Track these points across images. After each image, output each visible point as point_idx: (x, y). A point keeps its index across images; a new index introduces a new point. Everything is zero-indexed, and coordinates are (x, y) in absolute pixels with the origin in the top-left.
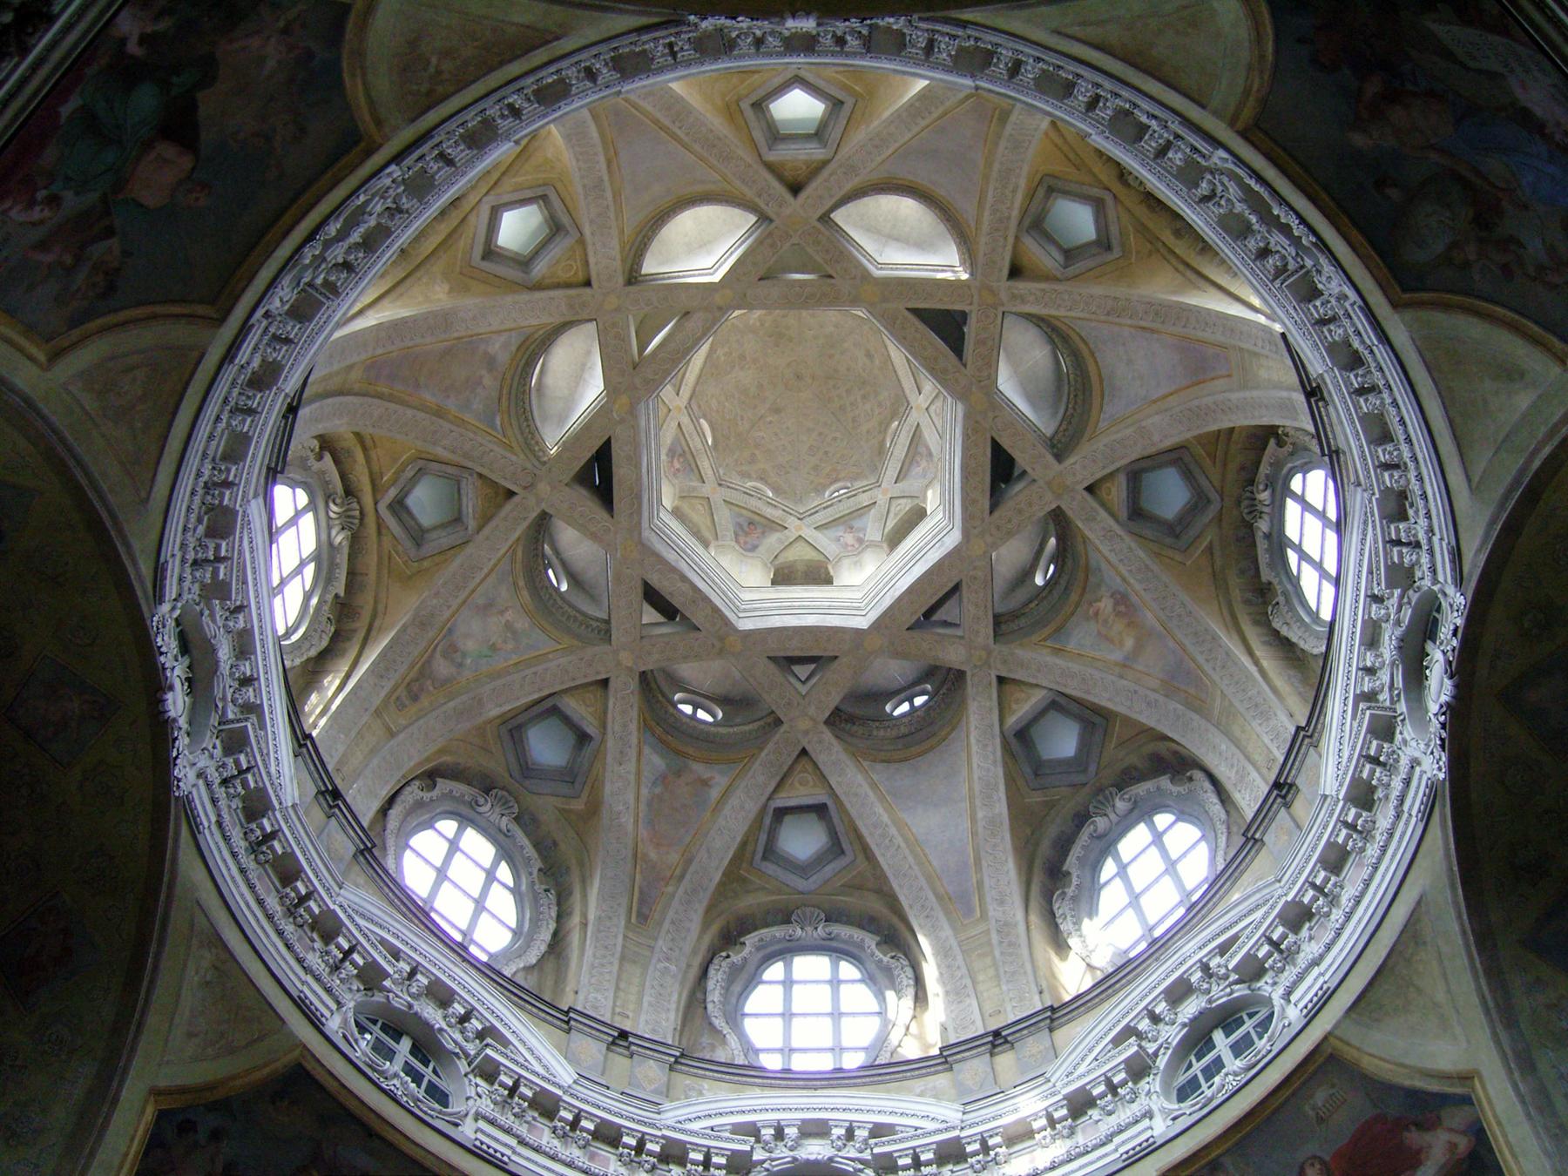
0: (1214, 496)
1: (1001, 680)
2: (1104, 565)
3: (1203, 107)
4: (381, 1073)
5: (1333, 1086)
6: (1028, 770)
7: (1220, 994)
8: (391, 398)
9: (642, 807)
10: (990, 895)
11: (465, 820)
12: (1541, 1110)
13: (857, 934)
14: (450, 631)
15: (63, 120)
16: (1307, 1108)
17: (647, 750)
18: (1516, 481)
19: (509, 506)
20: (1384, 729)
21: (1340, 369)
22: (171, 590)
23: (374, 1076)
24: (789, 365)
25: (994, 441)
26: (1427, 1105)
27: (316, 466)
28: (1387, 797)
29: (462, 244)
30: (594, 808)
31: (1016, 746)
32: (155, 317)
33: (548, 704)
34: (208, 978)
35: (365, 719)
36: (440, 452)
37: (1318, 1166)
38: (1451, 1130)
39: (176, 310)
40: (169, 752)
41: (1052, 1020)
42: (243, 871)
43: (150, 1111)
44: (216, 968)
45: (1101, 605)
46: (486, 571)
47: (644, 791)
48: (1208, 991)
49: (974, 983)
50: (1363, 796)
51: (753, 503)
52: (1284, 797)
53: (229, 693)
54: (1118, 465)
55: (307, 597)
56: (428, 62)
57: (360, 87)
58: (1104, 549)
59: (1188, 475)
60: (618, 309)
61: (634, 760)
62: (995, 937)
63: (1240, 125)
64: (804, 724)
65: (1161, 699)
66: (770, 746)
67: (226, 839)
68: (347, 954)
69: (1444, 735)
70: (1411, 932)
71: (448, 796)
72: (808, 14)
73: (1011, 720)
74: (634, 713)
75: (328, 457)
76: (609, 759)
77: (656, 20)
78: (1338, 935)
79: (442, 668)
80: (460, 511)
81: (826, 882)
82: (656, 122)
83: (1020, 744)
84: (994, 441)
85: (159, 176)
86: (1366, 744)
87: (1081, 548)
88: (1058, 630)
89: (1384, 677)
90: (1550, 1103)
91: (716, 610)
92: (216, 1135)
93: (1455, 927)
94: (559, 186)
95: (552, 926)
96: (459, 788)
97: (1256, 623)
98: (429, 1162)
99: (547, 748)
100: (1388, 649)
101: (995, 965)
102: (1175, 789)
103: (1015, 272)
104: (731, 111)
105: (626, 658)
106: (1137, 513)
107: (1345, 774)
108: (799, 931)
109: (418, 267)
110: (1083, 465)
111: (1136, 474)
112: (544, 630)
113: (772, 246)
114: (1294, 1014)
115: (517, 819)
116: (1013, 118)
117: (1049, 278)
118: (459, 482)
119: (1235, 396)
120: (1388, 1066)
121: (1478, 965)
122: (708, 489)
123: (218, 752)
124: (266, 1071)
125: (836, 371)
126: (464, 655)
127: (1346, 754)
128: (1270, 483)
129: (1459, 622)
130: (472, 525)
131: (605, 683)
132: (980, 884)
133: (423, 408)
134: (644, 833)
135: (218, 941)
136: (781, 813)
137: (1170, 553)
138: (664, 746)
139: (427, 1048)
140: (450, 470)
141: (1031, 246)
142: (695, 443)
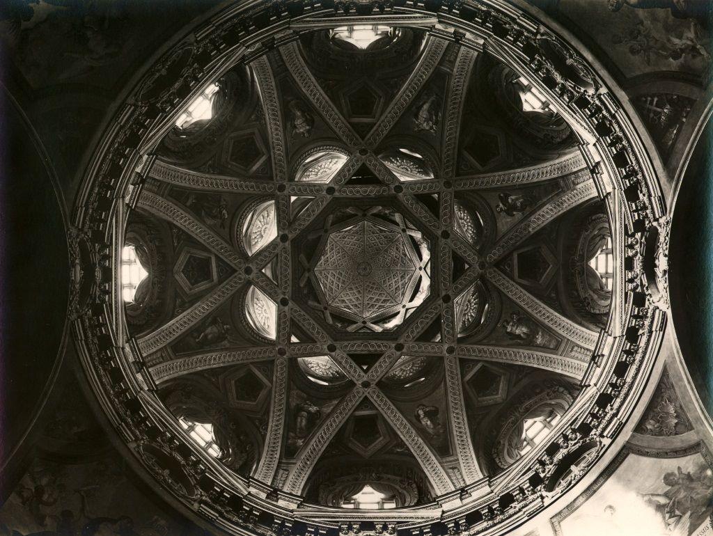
4: (166, 60)
7: (188, 471)
23: (166, 56)
48: (188, 465)
107: (306, 520)
130: (356, 120)
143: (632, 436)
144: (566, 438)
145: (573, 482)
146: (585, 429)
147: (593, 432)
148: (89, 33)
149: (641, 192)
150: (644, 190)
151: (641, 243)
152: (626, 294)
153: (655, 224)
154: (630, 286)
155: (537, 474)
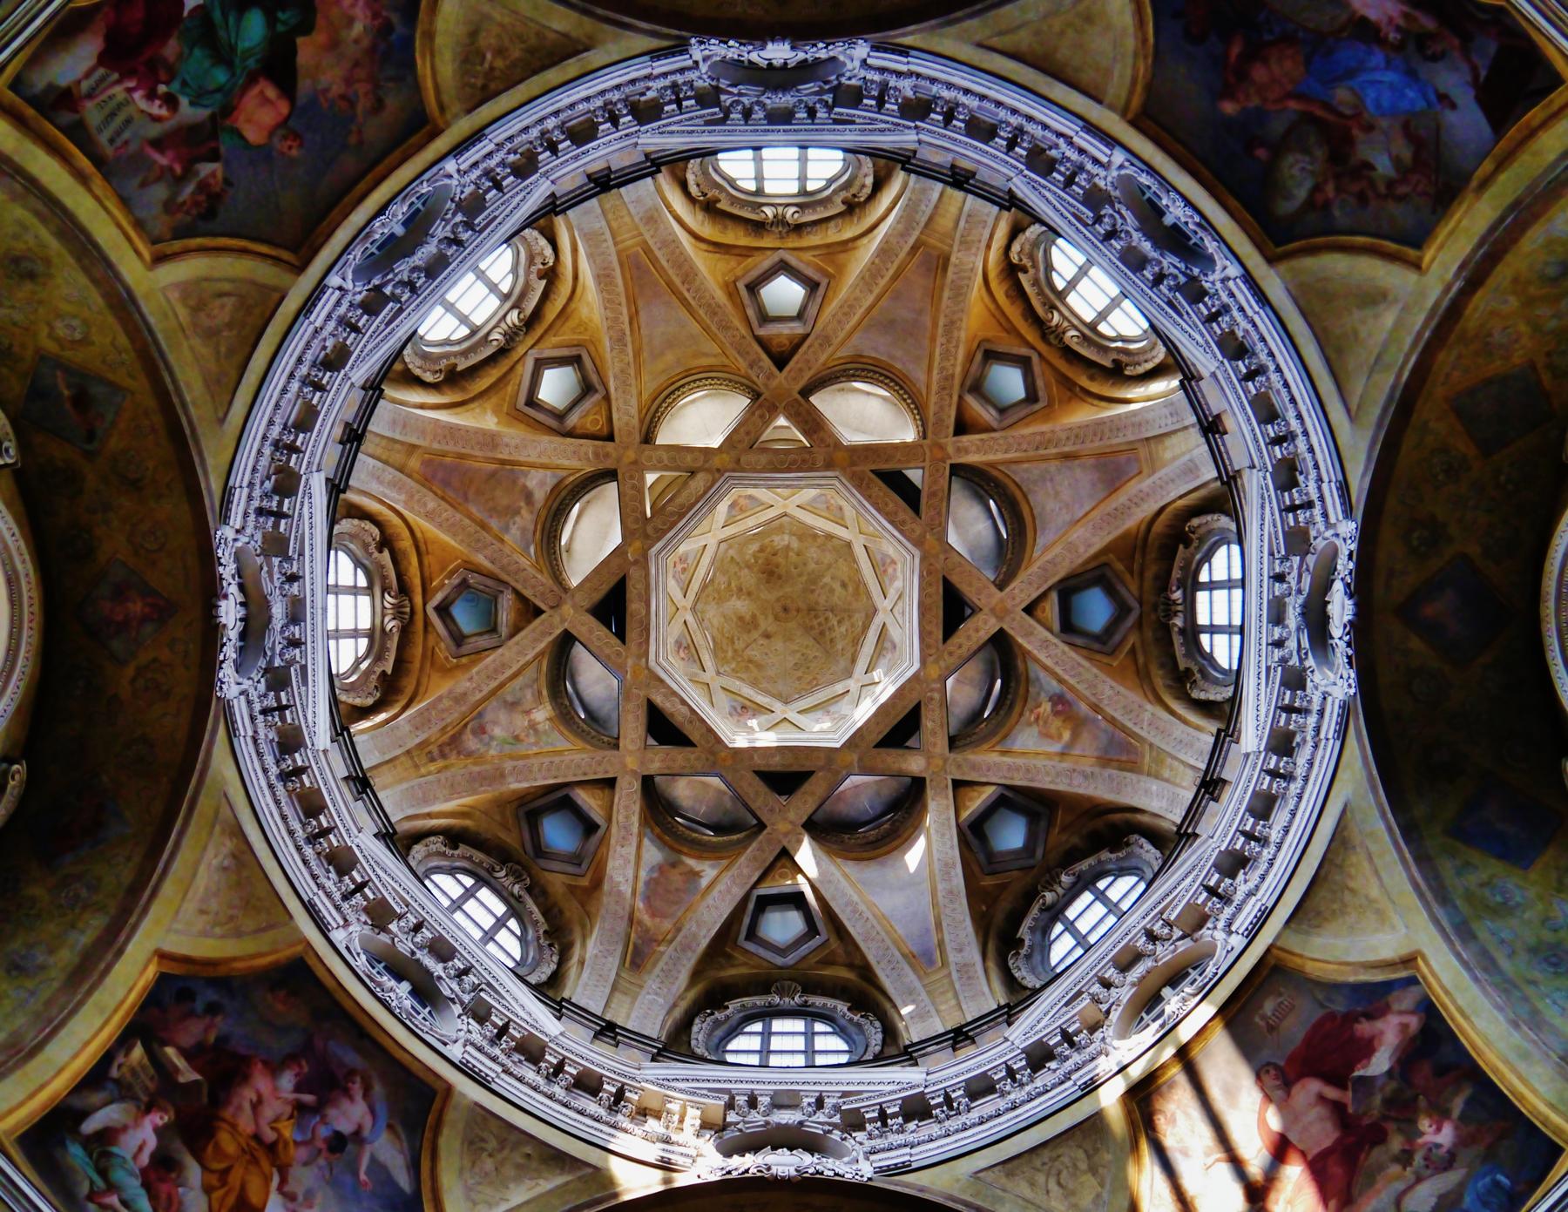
0: (1134, 604)
2: (1042, 674)
3: (1100, 102)
4: (379, 984)
5: (1280, 995)
6: (982, 857)
7: (1164, 953)
8: (443, 498)
9: (641, 885)
10: (949, 947)
11: (481, 881)
12: (1485, 970)
13: (830, 1002)
14: (480, 715)
15: (185, 14)
16: (1257, 1019)
17: (646, 842)
18: (1390, 397)
19: (537, 621)
20: (1295, 680)
21: (1230, 360)
22: (236, 519)
23: (371, 985)
24: (778, 600)
25: (945, 580)
27: (376, 554)
28: (1304, 740)
29: (510, 389)
30: (597, 883)
31: (970, 837)
32: (244, 251)
33: (559, 794)
34: (226, 863)
35: (399, 752)
36: (481, 559)
37: (1273, 1072)
38: (1401, 1013)
39: (264, 249)
40: (215, 657)
41: (1010, 1016)
42: (271, 786)
43: (151, 972)
44: (234, 856)
45: (1041, 710)
46: (514, 669)
47: (643, 874)
49: (938, 1011)
50: (1282, 744)
51: (747, 691)
52: (1212, 794)
53: (278, 648)
54: (1050, 583)
55: (358, 662)
56: (484, 57)
57: (428, 72)
58: (1042, 657)
59: (1111, 592)
60: (635, 462)
61: (634, 845)
62: (955, 975)
63: (1130, 116)
64: (783, 827)
65: (1097, 770)
66: (754, 845)
67: (260, 755)
68: (360, 888)
69: (1350, 652)
70: (1340, 839)
71: (470, 859)
72: (783, 39)
73: (965, 814)
74: (637, 808)
75: (386, 553)
76: (613, 841)
77: (665, 43)
78: (1271, 865)
79: (471, 742)
81: (804, 958)
82: (670, 284)
83: (974, 835)
84: (945, 580)
85: (259, 115)
86: (1280, 696)
87: (1020, 663)
88: (1005, 737)
89: (1292, 644)
90: (1492, 960)
91: (710, 730)
92: (213, 1009)
93: (1381, 826)
94: (592, 349)
95: (553, 967)
96: (478, 856)
97: (1178, 698)
98: (415, 1067)
99: (557, 834)
100: (1293, 618)
101: (956, 996)
102: (1113, 856)
104: (731, 290)
105: (631, 762)
106: (1068, 627)
108: (777, 999)
109: (472, 400)
110: (1023, 588)
111: (1068, 589)
112: (562, 733)
113: (762, 416)
114: (1237, 942)
115: (529, 890)
116: (953, 259)
117: (989, 429)
118: (494, 600)
119: (1146, 484)
120: (1331, 967)
121: (1408, 855)
122: (709, 675)
123: (262, 687)
125: (817, 603)
126: (492, 738)
128: (1181, 584)
129: (1353, 547)
131: (610, 783)
132: (941, 944)
133: (470, 516)
134: (640, 905)
135: (238, 832)
136: (766, 903)
137: (1098, 657)
138: (660, 841)
139: (426, 993)
141: (973, 403)
142: (698, 639)
143: (1111, 107)
144: (1111, 235)
145: (1197, 219)
146: (1095, 199)
147: (1102, 184)
148: (323, 1132)
149: (643, 94)
150: (640, 86)
151: (740, 94)
152: (836, 122)
153: (704, 68)
154: (822, 114)
155: (1178, 288)
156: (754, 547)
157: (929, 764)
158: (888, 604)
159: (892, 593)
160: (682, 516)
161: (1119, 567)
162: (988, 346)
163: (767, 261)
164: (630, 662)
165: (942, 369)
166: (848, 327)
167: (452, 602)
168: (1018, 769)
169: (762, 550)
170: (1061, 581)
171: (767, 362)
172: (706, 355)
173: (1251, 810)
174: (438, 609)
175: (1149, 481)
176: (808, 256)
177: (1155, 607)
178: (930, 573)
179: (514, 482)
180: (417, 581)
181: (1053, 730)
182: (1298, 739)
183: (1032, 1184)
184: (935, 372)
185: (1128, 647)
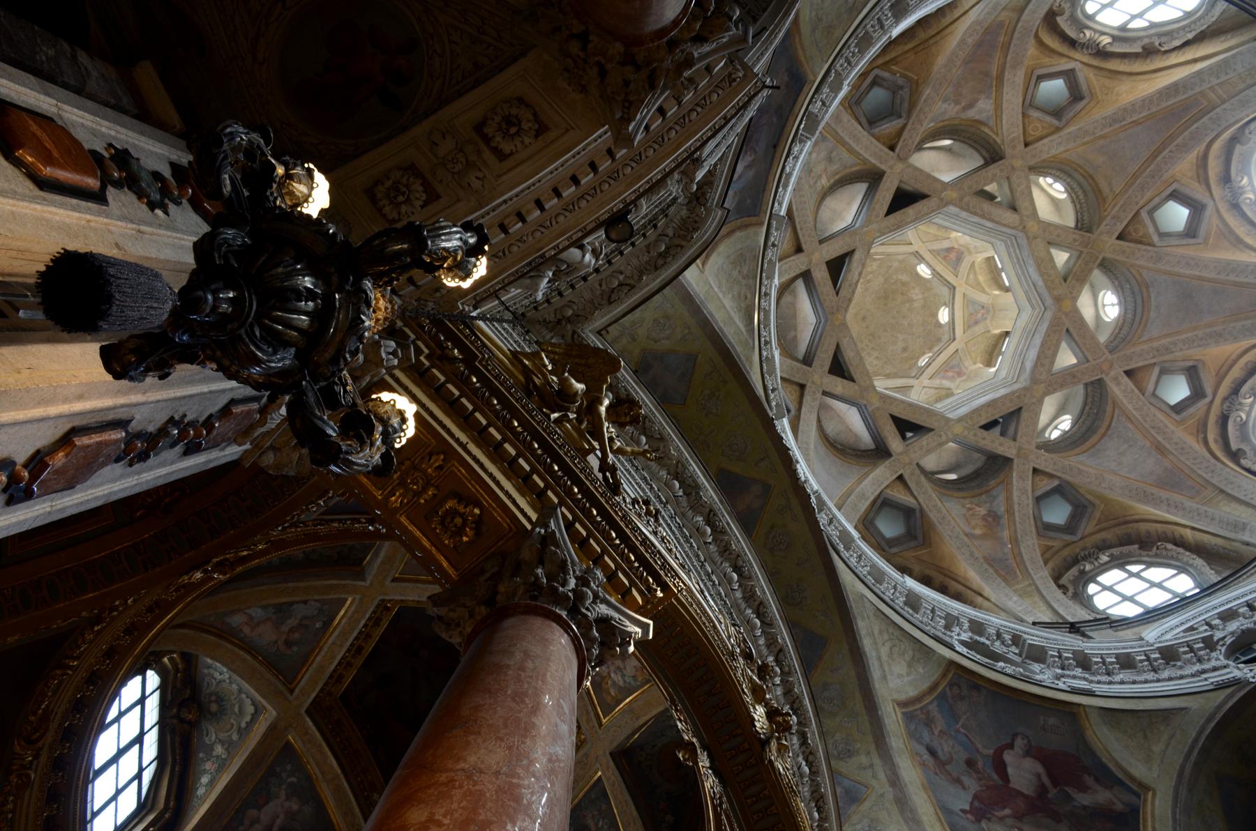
0: (1079, 535)
1: (900, 478)
19: (887, 150)
26: (1108, 777)
28: (1181, 668)
29: (1046, 60)
54: (1063, 476)
60: (1013, 169)
64: (816, 378)
80: (875, 122)
103: (1128, 373)
110: (1046, 461)
111: (1062, 490)
113: (1075, 240)
118: (892, 114)
124: (802, 59)
127: (1168, 637)
140: (906, 105)
141: (1156, 370)
156: (904, 278)
157: (901, 454)
158: (926, 382)
159: (937, 382)
160: (983, 216)
161: (1097, 515)
162: (1200, 366)
163: (1198, 193)
164: (875, 226)
165: (1175, 344)
166: (1176, 269)
167: (880, 86)
168: (939, 511)
169: (904, 284)
170: (1067, 482)
171: (1120, 227)
172: (1110, 184)
173: (1117, 656)
174: (877, 76)
175: (1194, 505)
176: (1215, 221)
177: (1084, 549)
178: (1019, 397)
179: (981, 92)
180: (893, 55)
181: (973, 522)
182: (1179, 663)
183: (881, 632)
184: (1169, 340)
185: (1050, 544)
